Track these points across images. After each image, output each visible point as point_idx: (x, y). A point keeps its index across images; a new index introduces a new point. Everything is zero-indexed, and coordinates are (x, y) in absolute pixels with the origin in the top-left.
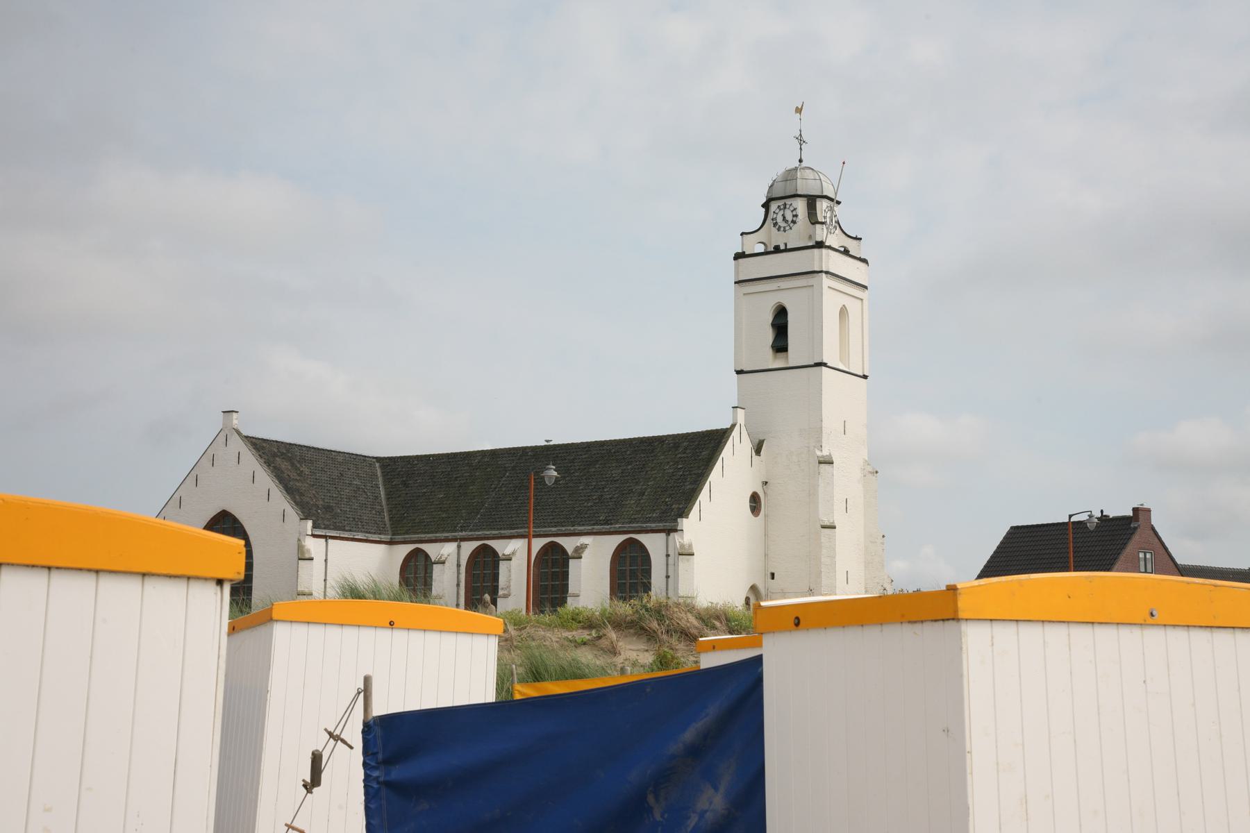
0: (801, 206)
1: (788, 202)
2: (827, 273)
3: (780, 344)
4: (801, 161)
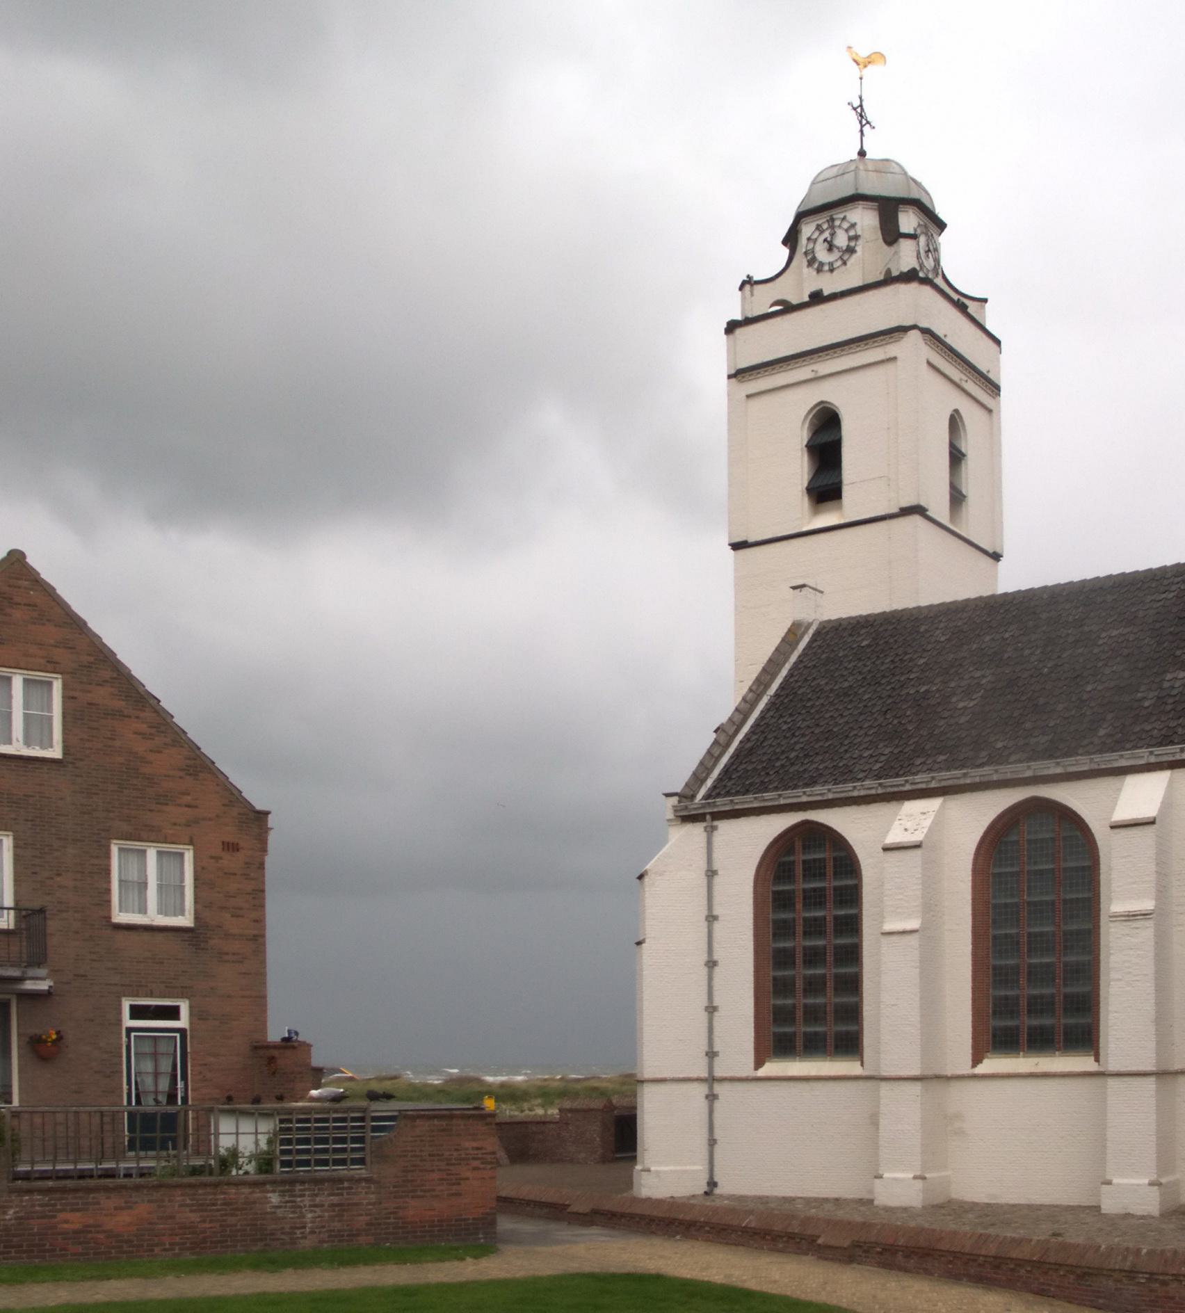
0: (865, 219)
1: (838, 214)
2: (926, 332)
3: (826, 480)
4: (862, 153)
